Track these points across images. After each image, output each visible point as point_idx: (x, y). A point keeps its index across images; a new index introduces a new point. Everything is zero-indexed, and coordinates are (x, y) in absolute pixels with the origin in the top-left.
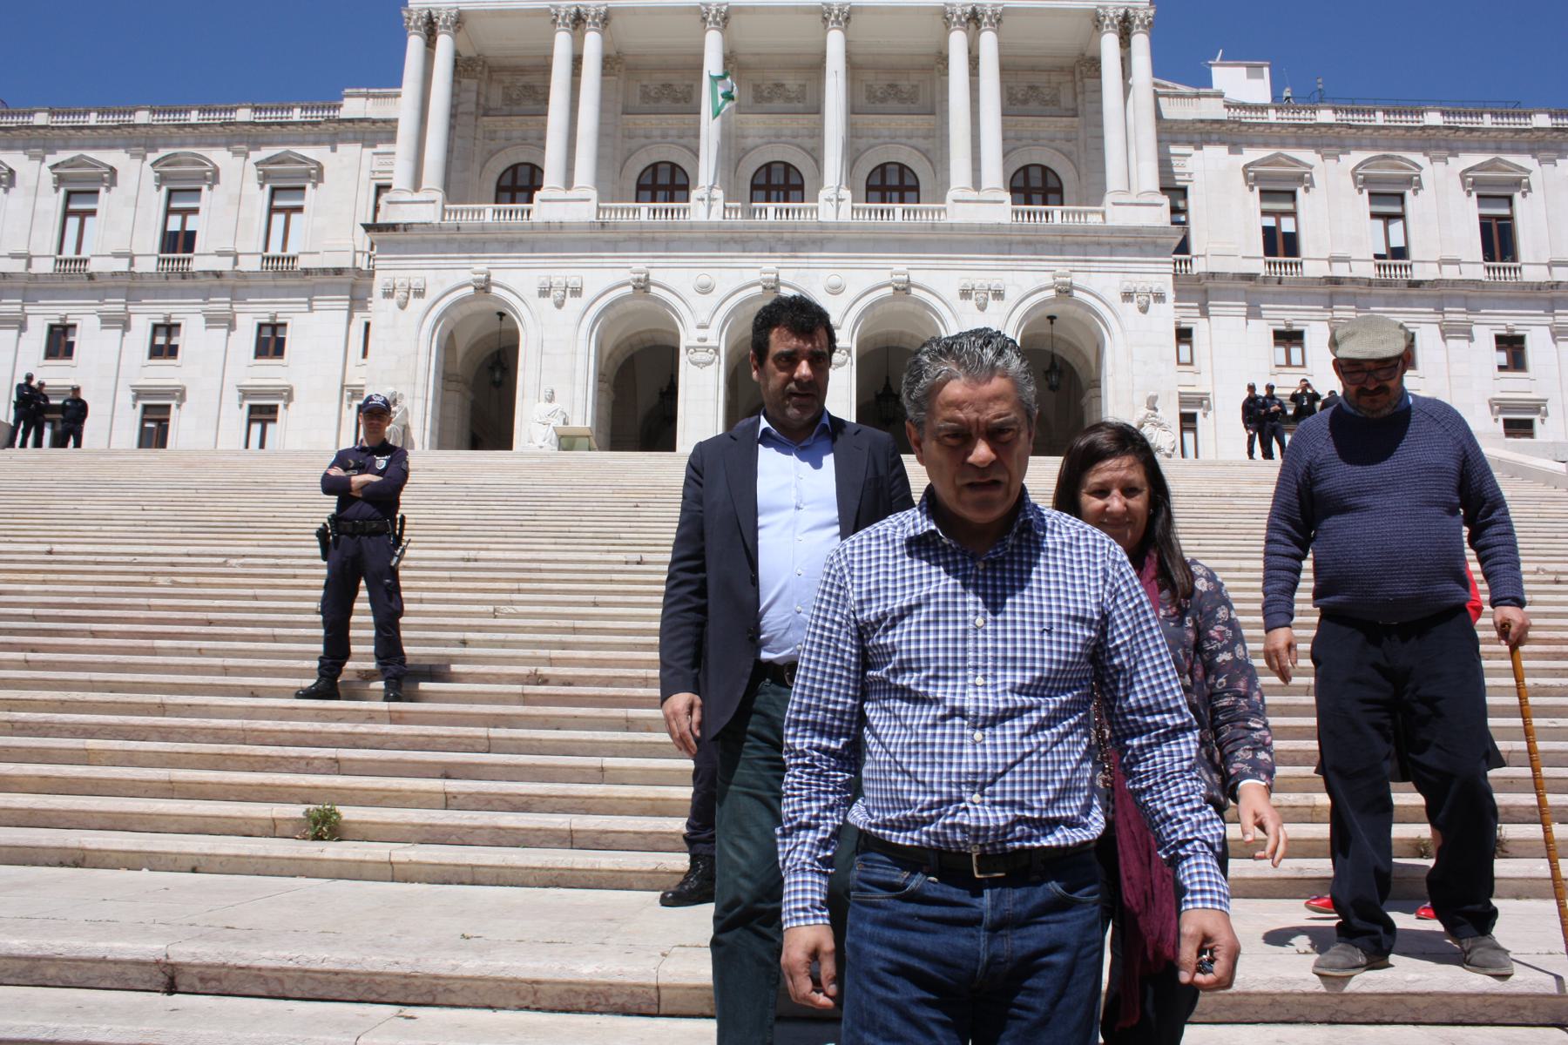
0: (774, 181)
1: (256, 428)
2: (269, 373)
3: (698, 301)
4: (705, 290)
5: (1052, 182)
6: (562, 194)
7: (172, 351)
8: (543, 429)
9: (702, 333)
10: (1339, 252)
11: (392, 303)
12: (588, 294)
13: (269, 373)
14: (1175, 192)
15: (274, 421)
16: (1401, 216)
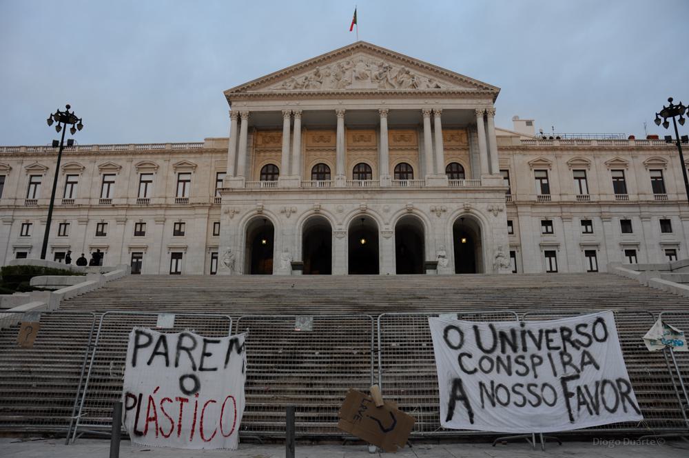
0: (361, 170)
1: (174, 261)
2: (179, 241)
3: (338, 216)
4: (341, 211)
5: (460, 169)
6: (288, 177)
7: (141, 233)
8: (285, 262)
9: (340, 227)
10: (563, 192)
11: (228, 217)
12: (299, 213)
13: (179, 241)
14: (506, 173)
15: (181, 258)
16: (585, 178)
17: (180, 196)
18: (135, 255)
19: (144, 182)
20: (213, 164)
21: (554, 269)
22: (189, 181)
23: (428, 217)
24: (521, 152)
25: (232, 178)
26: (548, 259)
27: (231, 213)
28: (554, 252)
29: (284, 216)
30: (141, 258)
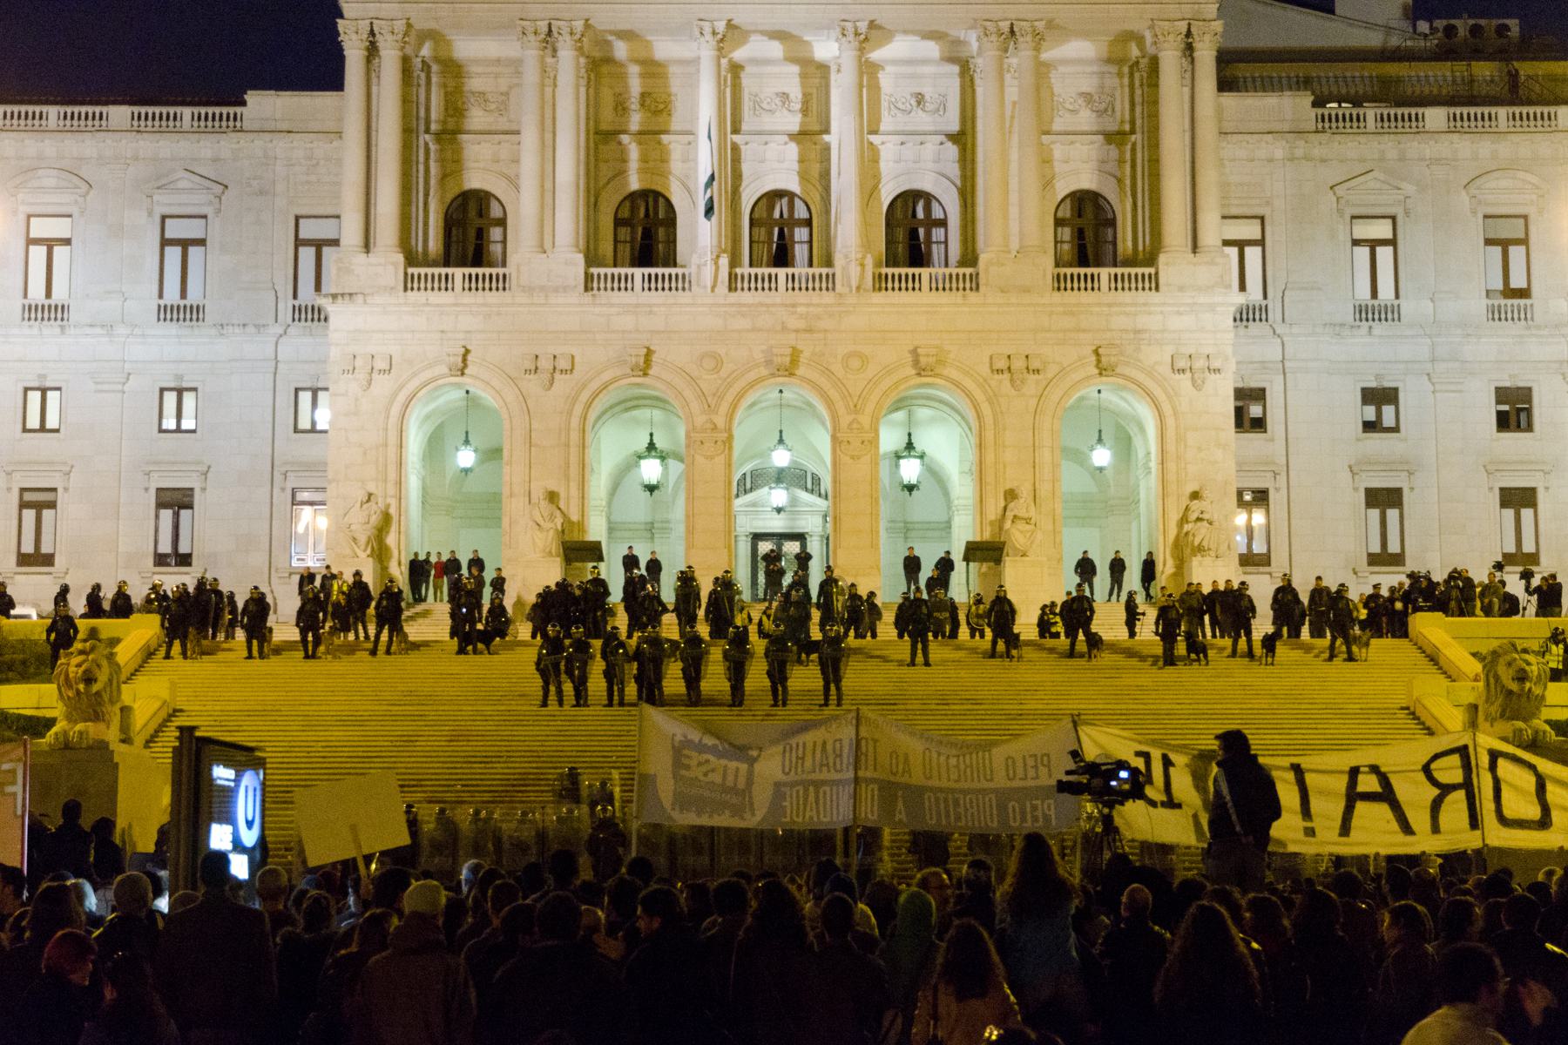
1: (167, 515)
15: (190, 506)
17: (172, 295)
18: (28, 497)
19: (37, 241)
20: (280, 187)
21: (1393, 547)
22: (201, 242)
23: (985, 392)
24: (1317, 152)
25: (362, 257)
26: (1375, 514)
27: (361, 375)
28: (1397, 492)
29: (533, 384)
30: (52, 505)
